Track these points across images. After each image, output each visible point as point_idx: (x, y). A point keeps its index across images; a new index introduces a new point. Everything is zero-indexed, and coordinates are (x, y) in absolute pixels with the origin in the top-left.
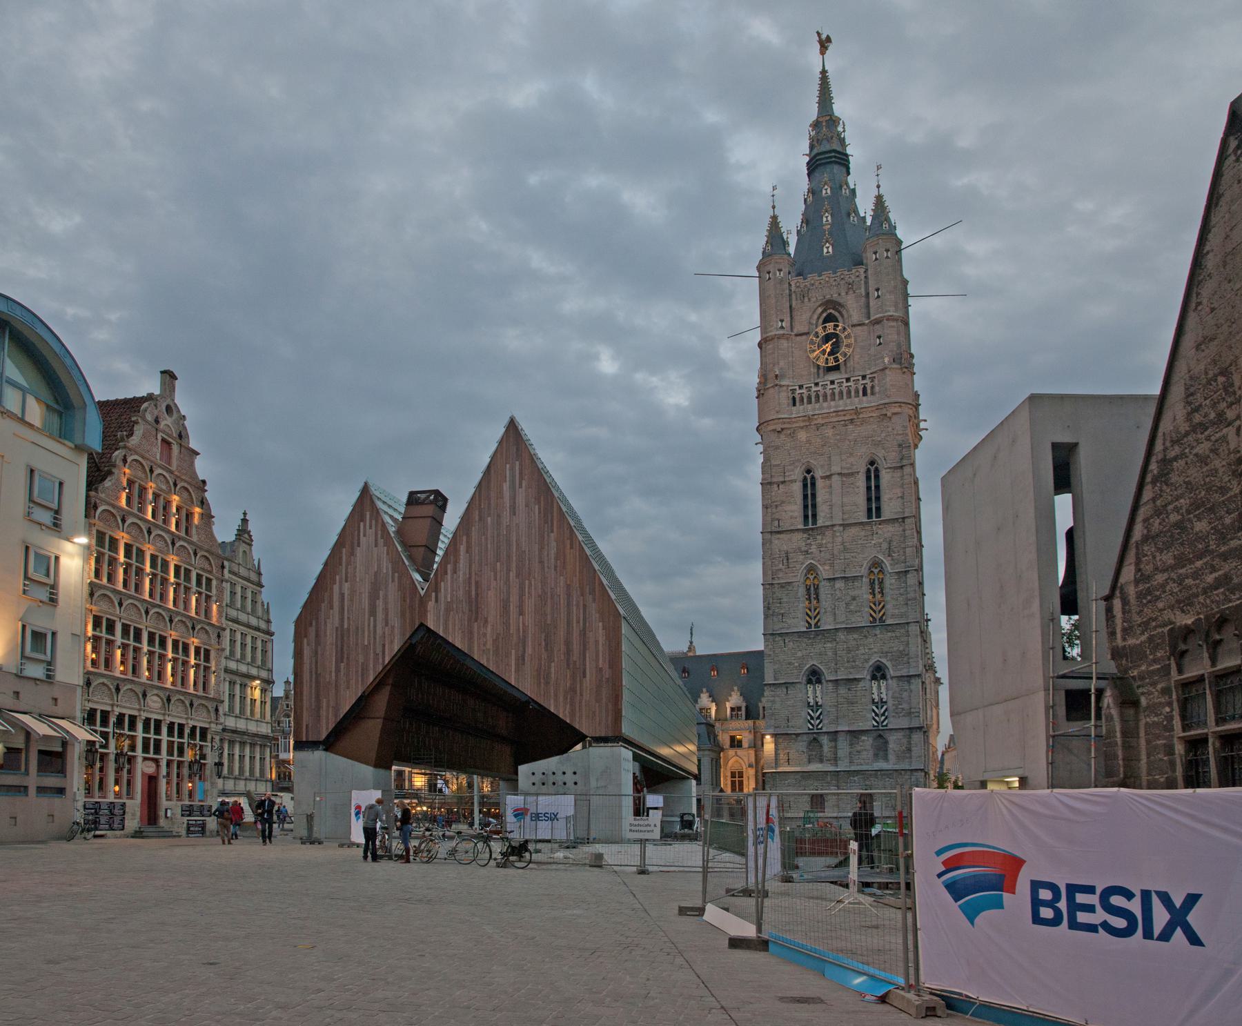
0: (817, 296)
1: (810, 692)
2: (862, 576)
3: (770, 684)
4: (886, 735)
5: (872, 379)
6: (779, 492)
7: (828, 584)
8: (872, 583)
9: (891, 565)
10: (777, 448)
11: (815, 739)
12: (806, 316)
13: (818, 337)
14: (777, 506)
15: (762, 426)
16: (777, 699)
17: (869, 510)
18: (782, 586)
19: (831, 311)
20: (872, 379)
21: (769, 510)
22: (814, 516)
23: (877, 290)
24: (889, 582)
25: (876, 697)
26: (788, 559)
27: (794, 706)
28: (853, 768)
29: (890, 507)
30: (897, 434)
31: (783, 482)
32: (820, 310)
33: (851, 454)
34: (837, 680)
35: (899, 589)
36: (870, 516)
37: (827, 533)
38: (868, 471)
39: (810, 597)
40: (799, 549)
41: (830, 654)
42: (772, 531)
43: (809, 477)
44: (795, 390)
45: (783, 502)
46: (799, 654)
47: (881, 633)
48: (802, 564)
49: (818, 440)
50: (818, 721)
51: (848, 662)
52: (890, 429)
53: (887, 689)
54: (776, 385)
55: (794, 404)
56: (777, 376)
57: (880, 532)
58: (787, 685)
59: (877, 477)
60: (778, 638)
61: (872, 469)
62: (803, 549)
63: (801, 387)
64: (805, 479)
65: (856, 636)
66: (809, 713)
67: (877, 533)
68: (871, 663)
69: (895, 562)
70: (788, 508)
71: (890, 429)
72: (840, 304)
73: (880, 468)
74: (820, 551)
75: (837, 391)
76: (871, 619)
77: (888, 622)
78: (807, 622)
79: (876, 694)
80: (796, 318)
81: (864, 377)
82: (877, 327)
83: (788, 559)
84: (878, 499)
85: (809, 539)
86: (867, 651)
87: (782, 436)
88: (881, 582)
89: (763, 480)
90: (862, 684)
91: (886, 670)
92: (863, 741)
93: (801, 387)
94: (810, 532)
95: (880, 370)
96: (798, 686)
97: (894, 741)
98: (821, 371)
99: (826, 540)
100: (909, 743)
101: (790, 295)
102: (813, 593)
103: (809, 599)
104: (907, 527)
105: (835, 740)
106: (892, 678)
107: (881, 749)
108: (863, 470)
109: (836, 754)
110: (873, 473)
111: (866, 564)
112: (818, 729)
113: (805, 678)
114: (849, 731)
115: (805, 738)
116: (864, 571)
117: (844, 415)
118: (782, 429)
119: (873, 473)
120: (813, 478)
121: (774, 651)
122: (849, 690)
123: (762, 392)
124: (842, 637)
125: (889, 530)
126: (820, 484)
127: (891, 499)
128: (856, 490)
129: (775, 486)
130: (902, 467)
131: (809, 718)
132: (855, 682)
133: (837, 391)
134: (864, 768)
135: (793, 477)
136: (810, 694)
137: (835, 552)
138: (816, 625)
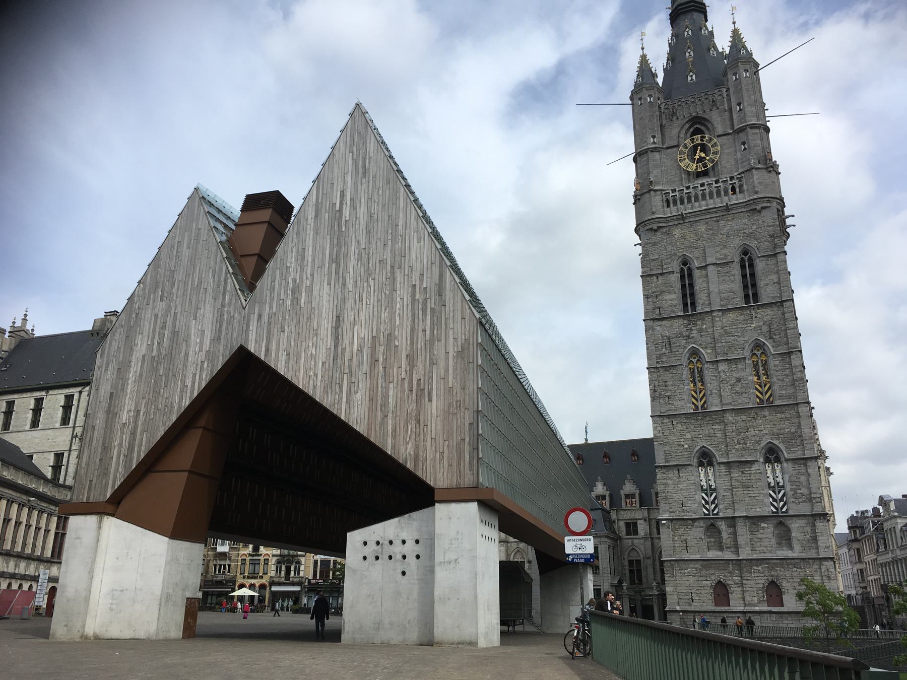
0: (685, 114)
1: (702, 475)
2: (745, 358)
3: (661, 467)
4: (788, 522)
5: (740, 179)
6: (658, 283)
7: (711, 367)
8: (756, 366)
9: (773, 346)
10: (654, 244)
11: (712, 525)
12: (675, 131)
13: (687, 148)
14: (657, 296)
15: (639, 227)
16: (669, 482)
17: (747, 297)
18: (667, 369)
19: (698, 126)
20: (740, 179)
21: (650, 300)
22: (693, 304)
23: (739, 104)
24: (773, 363)
25: (771, 480)
26: (670, 344)
27: (687, 490)
28: (755, 556)
29: (767, 293)
30: (768, 226)
31: (662, 274)
32: (687, 126)
33: (725, 246)
34: (729, 463)
35: (784, 370)
36: (747, 301)
37: (706, 319)
38: (742, 260)
39: (694, 379)
40: (681, 333)
41: (719, 435)
42: (654, 318)
43: (685, 268)
44: (669, 193)
45: (663, 292)
46: (688, 436)
47: (770, 414)
48: (685, 348)
49: (692, 236)
50: (713, 506)
51: (739, 444)
52: (760, 222)
53: (783, 473)
54: (651, 190)
55: (668, 206)
56: (651, 182)
57: (759, 316)
58: (679, 467)
59: (751, 266)
60: (666, 420)
61: (746, 258)
62: (685, 334)
63: (674, 191)
64: (682, 270)
65: (744, 418)
66: (703, 498)
67: (756, 317)
68: (762, 445)
69: (776, 345)
70: (668, 297)
71: (760, 222)
72: (705, 119)
73: (754, 257)
74: (701, 336)
75: (707, 191)
76: (758, 400)
77: (777, 403)
78: (694, 404)
79: (771, 477)
80: (667, 134)
81: (732, 178)
82: (741, 135)
83: (670, 344)
84: (754, 285)
85: (689, 325)
86: (757, 432)
87: (659, 234)
88: (765, 364)
89: (643, 272)
90: (755, 467)
91: (780, 453)
92: (763, 528)
93: (674, 191)
94: (690, 318)
95: (747, 171)
96: (690, 468)
97: (797, 528)
98: (691, 177)
99: (706, 325)
100: (814, 531)
101: (660, 116)
102: (697, 376)
103: (694, 382)
104: (786, 310)
105: (734, 526)
106: (787, 460)
107: (785, 538)
108: (737, 259)
109: (736, 540)
110: (747, 261)
111: (748, 348)
112: (713, 515)
113: (695, 460)
114: (747, 517)
115: (702, 523)
116: (747, 353)
117: (716, 212)
118: (659, 228)
119: (747, 261)
120: (690, 269)
121: (663, 433)
122: (742, 472)
123: (638, 197)
124: (730, 418)
125: (768, 314)
126: (697, 274)
127: (767, 285)
128: (732, 278)
129: (655, 278)
130: (775, 255)
131: (703, 502)
132: (749, 465)
133: (707, 191)
134: (768, 556)
135: (670, 269)
136: (702, 477)
137: (716, 336)
138: (702, 406)
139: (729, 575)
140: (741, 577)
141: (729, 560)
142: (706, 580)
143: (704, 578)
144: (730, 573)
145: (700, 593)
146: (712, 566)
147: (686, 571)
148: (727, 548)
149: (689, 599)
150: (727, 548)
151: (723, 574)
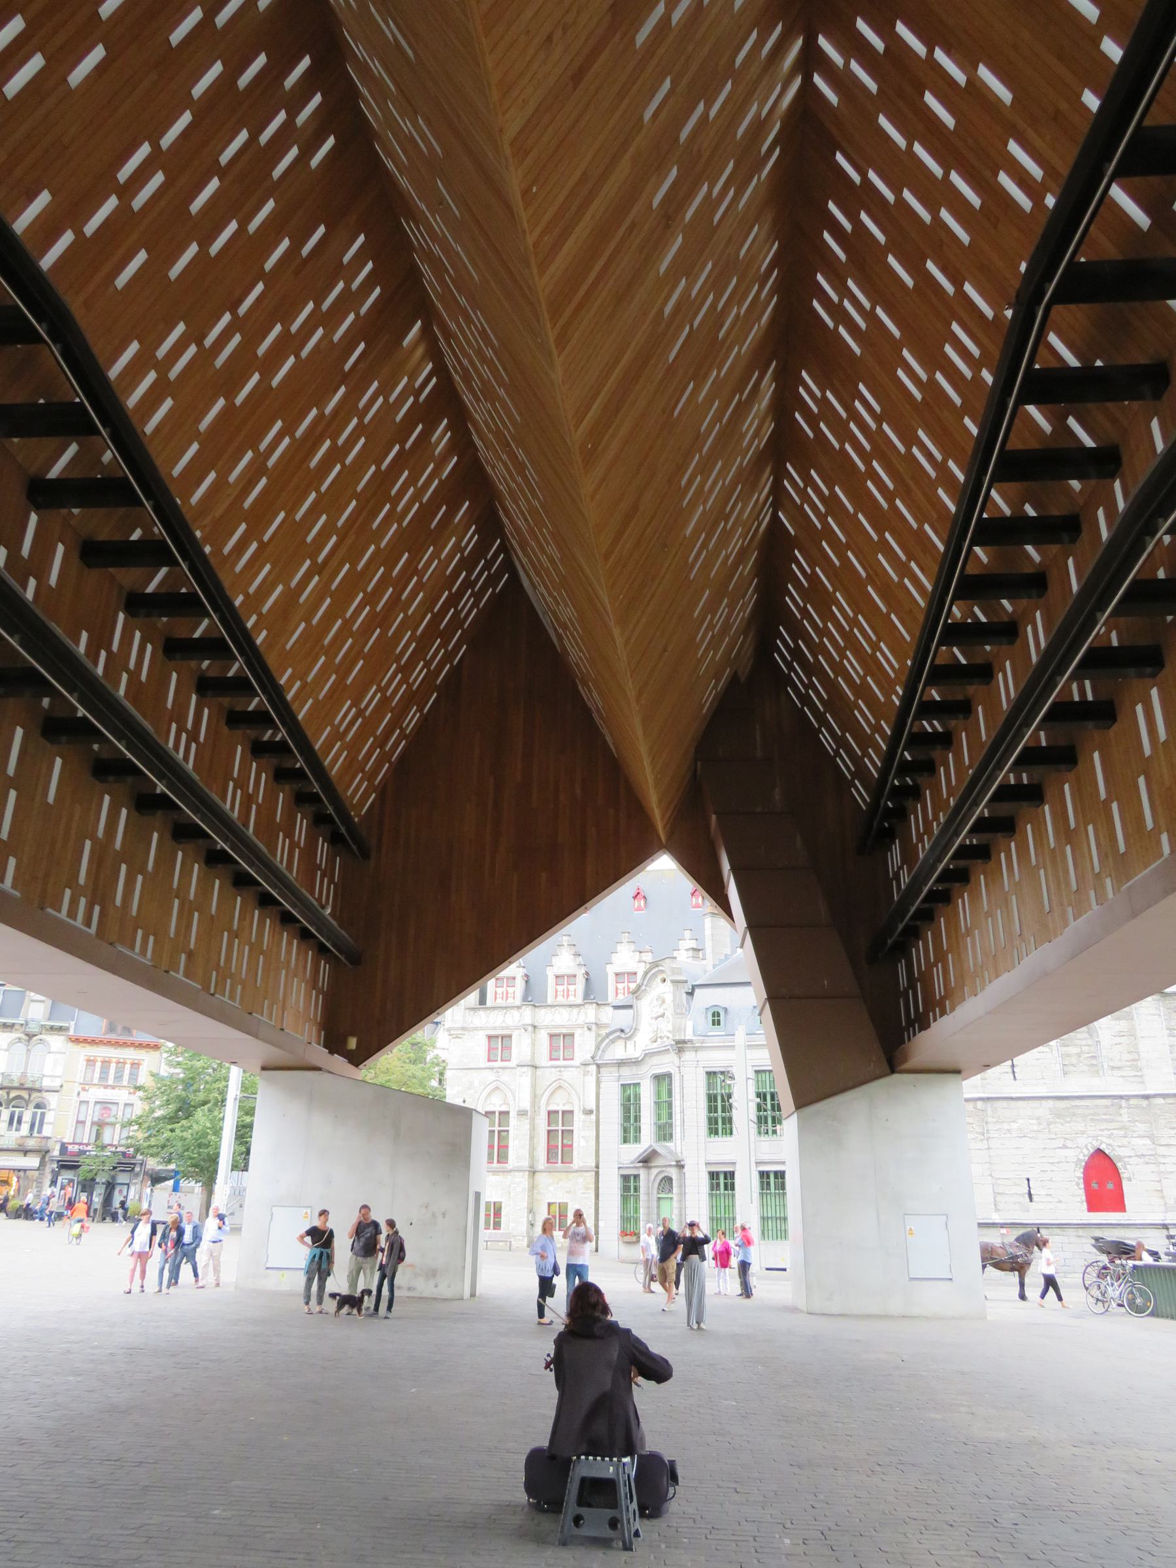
139: (1122, 1133)
140: (1151, 1137)
141: (1121, 1097)
142: (1065, 1147)
143: (1060, 1143)
144: (1123, 1128)
145: (1051, 1180)
146: (1079, 1111)
147: (1014, 1126)
148: (1113, 1068)
149: (1022, 1195)
150: (1113, 1068)
151: (1106, 1132)
